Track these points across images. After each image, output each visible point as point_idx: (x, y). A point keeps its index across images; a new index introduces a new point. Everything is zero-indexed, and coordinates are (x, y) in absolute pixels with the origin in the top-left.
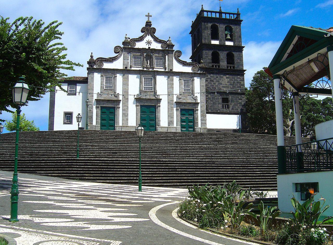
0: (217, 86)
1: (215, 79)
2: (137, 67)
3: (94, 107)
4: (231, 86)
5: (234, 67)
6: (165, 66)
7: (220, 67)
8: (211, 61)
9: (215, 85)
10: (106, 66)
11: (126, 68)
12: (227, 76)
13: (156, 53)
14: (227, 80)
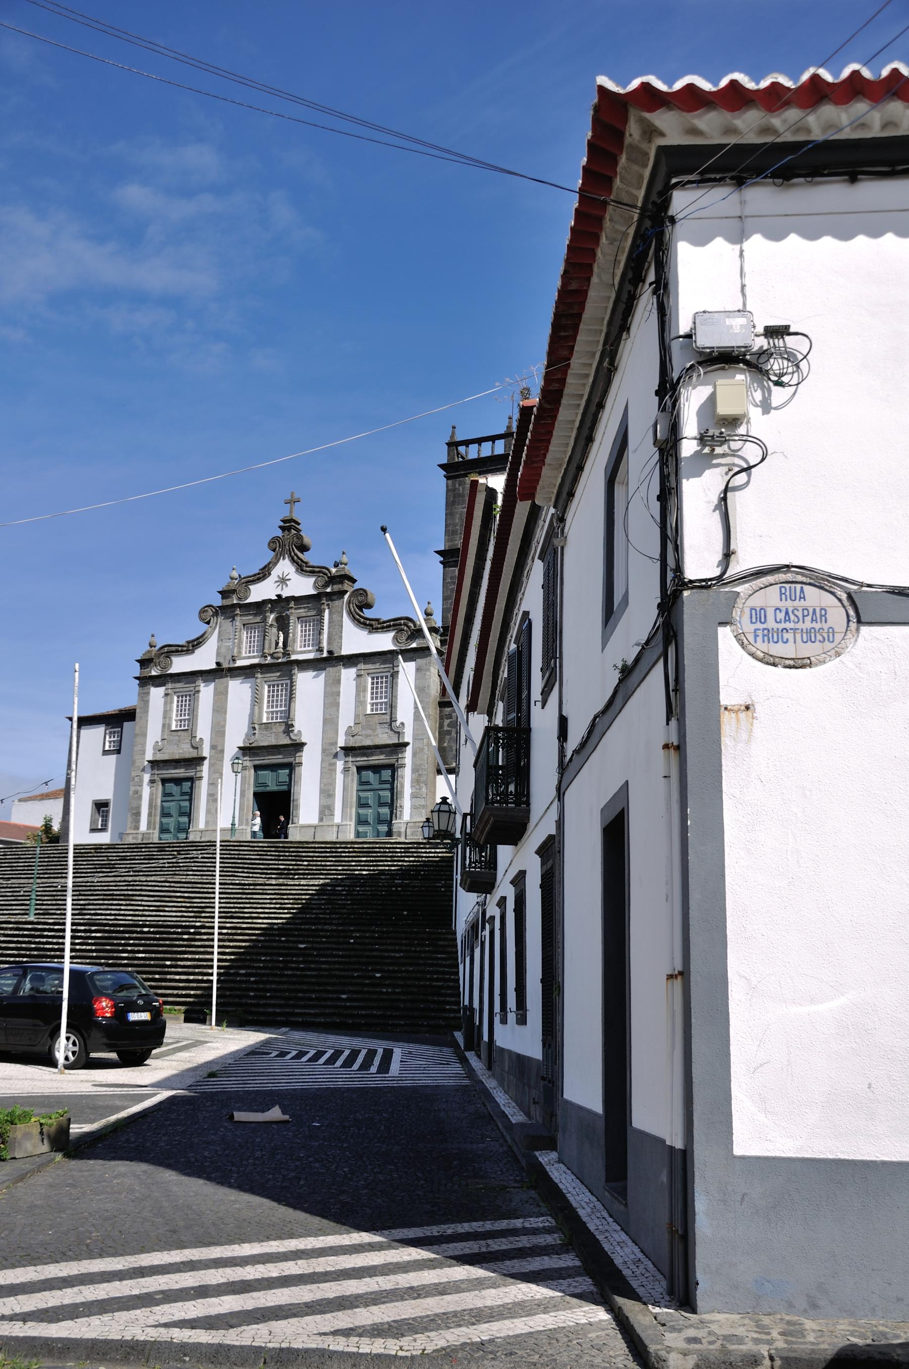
2: (249, 658)
10: (180, 664)
11: (218, 664)
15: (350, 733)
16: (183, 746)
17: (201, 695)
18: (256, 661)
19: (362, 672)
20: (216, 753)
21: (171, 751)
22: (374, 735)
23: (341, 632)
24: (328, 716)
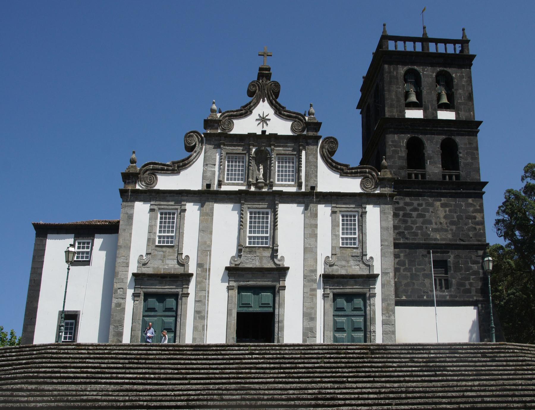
0: (421, 228)
1: (415, 210)
2: (233, 184)
3: (130, 292)
4: (454, 227)
5: (458, 177)
6: (299, 177)
7: (427, 177)
8: (404, 163)
9: (414, 227)
11: (209, 186)
12: (444, 200)
13: (279, 146)
14: (441, 213)
15: (328, 263)
16: (168, 262)
17: (187, 214)
18: (244, 188)
19: (336, 210)
20: (202, 271)
21: (156, 266)
22: (348, 266)
23: (317, 172)
24: (307, 246)
